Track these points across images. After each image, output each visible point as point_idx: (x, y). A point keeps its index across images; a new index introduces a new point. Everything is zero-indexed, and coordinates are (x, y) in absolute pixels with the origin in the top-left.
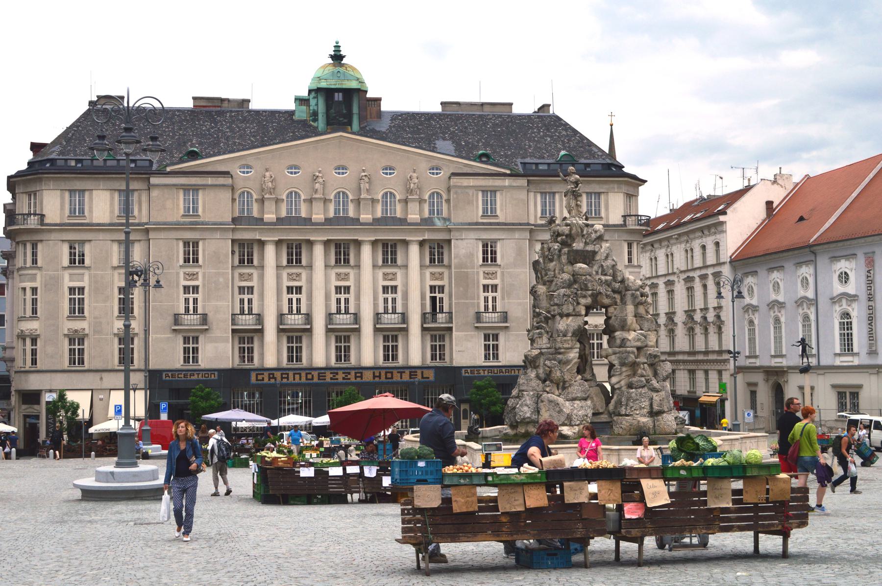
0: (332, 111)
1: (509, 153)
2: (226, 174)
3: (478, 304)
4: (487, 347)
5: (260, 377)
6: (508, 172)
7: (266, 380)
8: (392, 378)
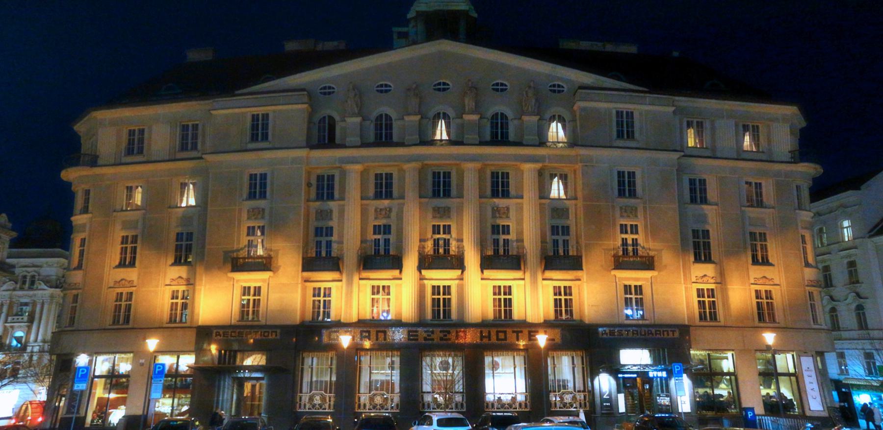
8: (505, 339)
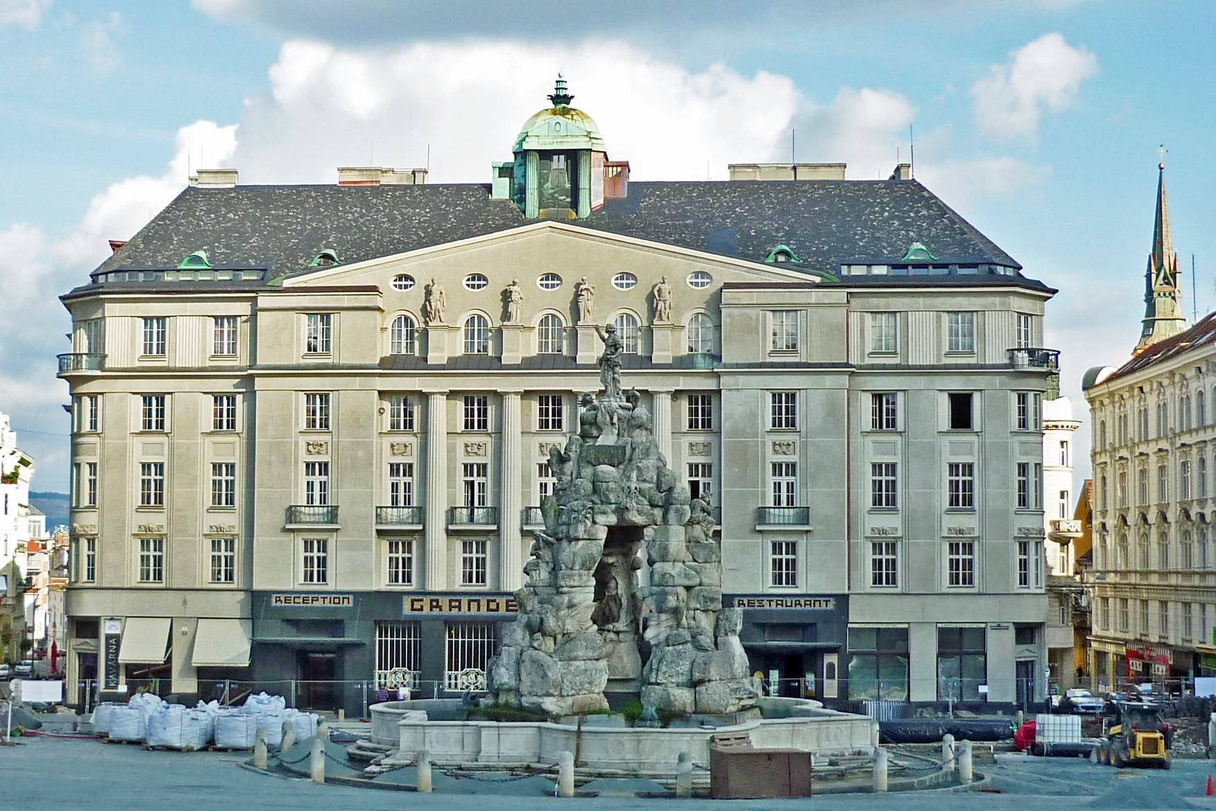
0: (549, 185)
1: (826, 248)
2: (373, 289)
3: (764, 494)
4: (777, 564)
5: (417, 605)
6: (818, 280)
7: (426, 610)
